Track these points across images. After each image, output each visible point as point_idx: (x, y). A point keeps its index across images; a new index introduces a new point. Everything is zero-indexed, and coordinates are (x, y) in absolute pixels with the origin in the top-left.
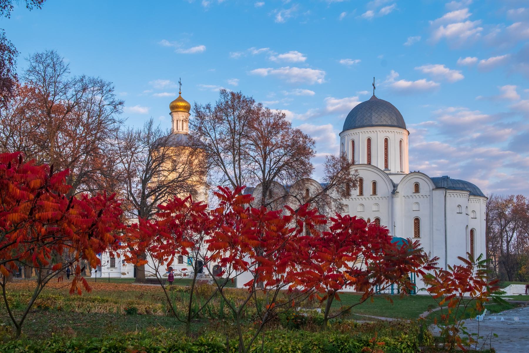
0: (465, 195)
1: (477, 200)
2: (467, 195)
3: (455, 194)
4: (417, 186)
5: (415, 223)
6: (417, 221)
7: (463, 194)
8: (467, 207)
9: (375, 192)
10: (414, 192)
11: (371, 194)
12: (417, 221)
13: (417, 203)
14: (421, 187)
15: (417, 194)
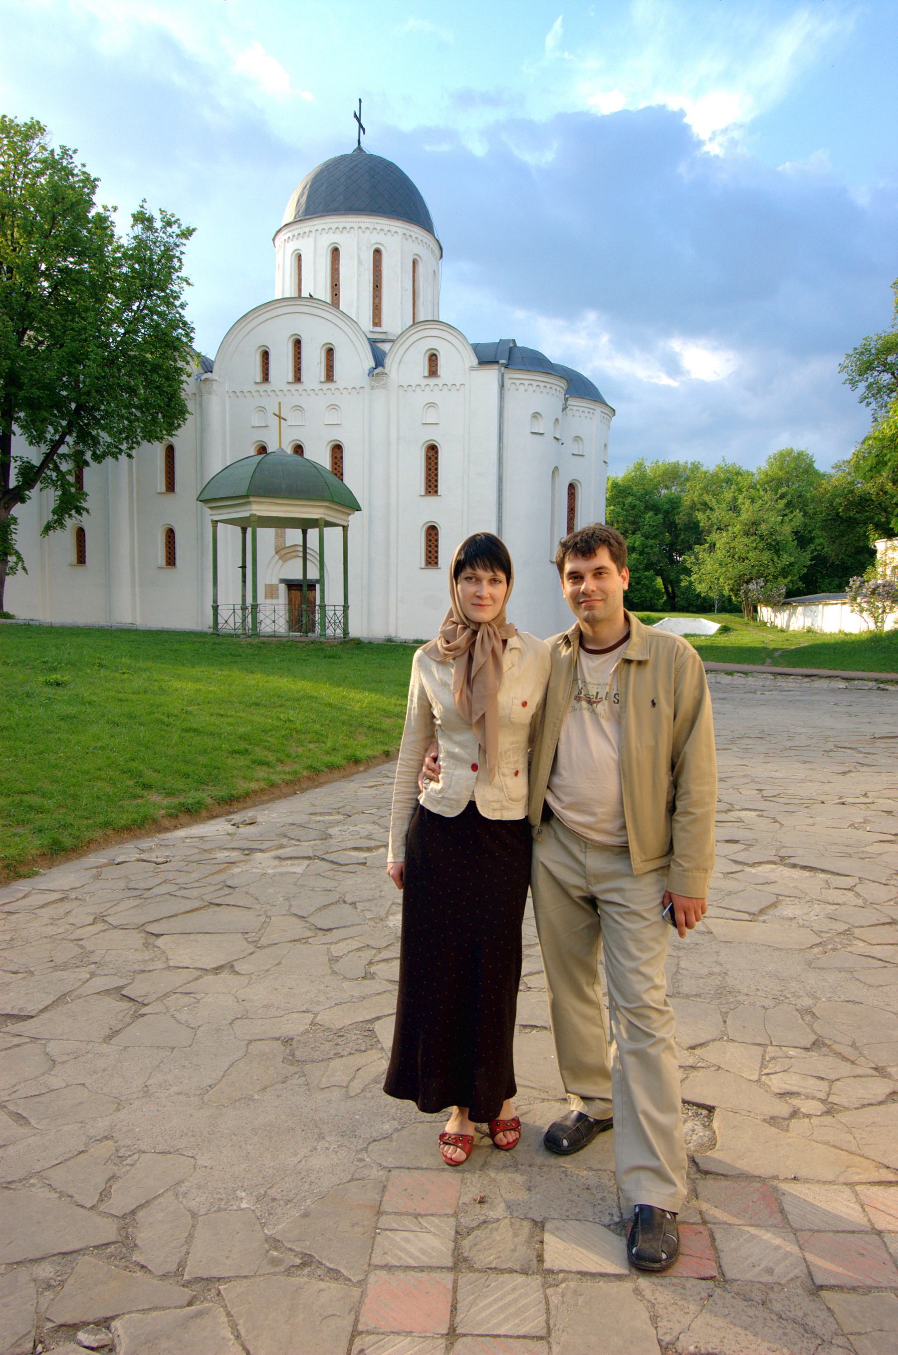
0: (554, 387)
1: (587, 410)
2: (559, 389)
3: (527, 383)
4: (433, 359)
5: (428, 458)
6: (432, 450)
7: (548, 386)
8: (557, 420)
9: (330, 375)
10: (427, 374)
11: (323, 379)
12: (432, 450)
13: (432, 405)
14: (441, 361)
15: (433, 381)
